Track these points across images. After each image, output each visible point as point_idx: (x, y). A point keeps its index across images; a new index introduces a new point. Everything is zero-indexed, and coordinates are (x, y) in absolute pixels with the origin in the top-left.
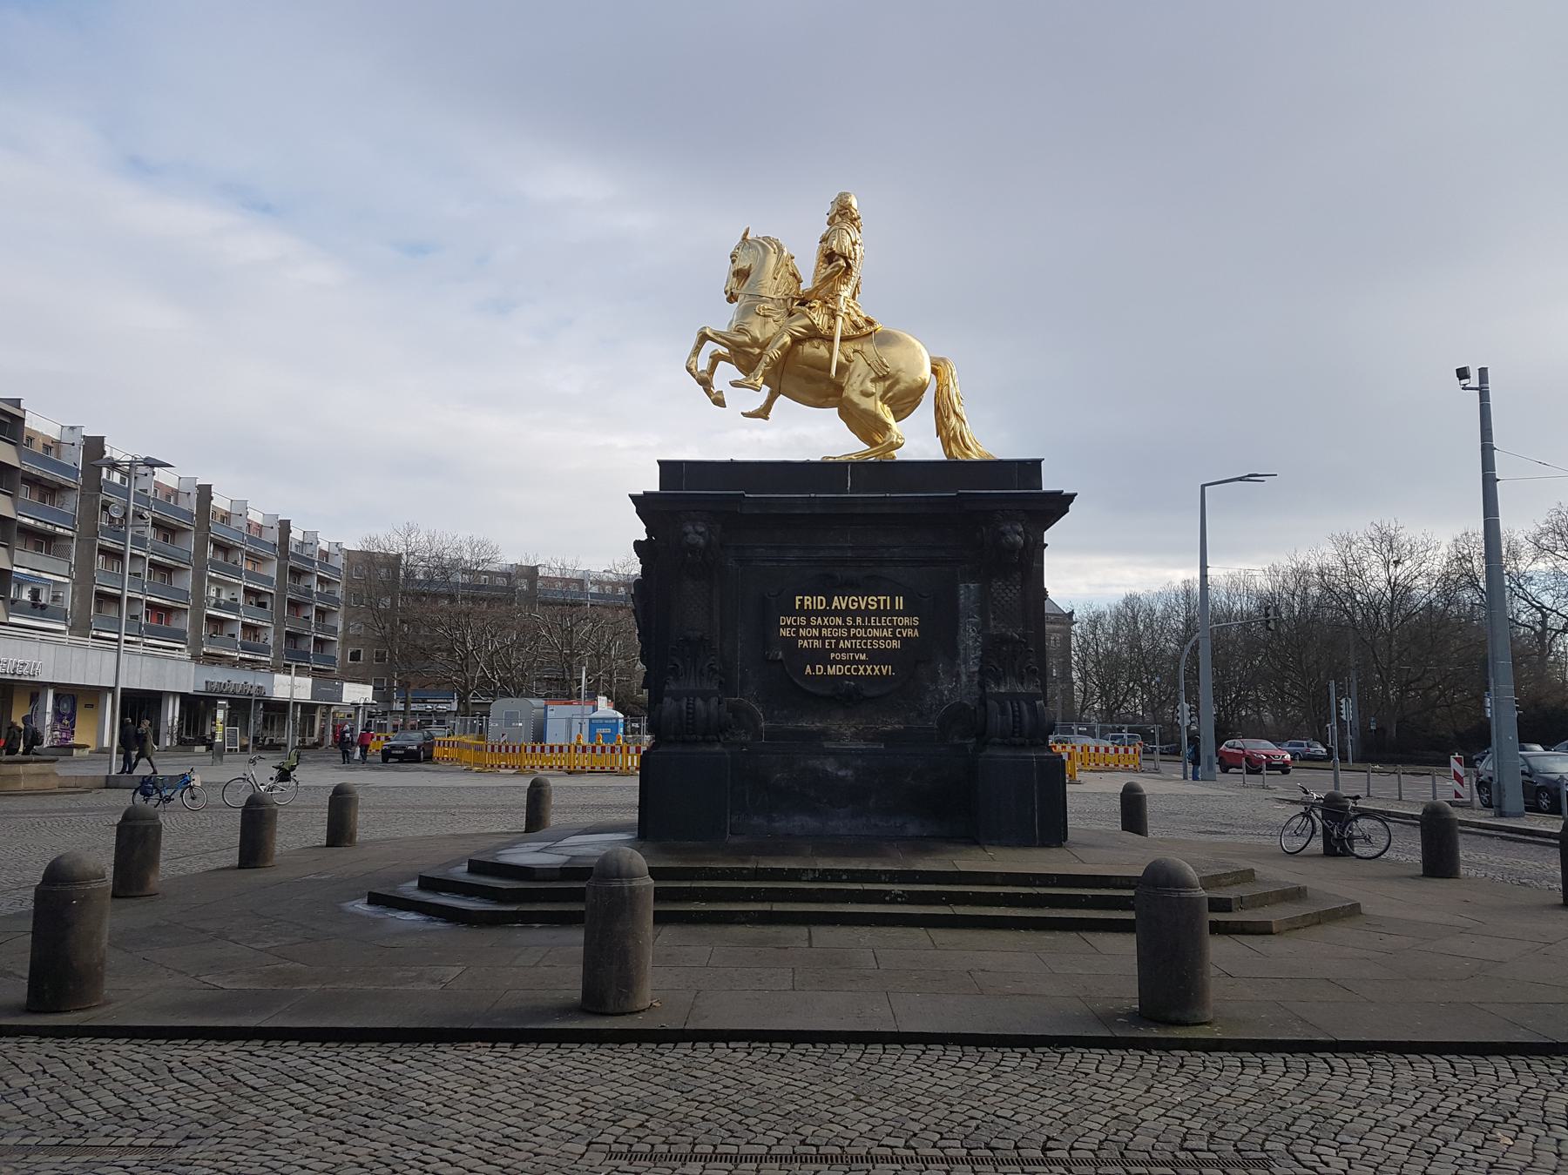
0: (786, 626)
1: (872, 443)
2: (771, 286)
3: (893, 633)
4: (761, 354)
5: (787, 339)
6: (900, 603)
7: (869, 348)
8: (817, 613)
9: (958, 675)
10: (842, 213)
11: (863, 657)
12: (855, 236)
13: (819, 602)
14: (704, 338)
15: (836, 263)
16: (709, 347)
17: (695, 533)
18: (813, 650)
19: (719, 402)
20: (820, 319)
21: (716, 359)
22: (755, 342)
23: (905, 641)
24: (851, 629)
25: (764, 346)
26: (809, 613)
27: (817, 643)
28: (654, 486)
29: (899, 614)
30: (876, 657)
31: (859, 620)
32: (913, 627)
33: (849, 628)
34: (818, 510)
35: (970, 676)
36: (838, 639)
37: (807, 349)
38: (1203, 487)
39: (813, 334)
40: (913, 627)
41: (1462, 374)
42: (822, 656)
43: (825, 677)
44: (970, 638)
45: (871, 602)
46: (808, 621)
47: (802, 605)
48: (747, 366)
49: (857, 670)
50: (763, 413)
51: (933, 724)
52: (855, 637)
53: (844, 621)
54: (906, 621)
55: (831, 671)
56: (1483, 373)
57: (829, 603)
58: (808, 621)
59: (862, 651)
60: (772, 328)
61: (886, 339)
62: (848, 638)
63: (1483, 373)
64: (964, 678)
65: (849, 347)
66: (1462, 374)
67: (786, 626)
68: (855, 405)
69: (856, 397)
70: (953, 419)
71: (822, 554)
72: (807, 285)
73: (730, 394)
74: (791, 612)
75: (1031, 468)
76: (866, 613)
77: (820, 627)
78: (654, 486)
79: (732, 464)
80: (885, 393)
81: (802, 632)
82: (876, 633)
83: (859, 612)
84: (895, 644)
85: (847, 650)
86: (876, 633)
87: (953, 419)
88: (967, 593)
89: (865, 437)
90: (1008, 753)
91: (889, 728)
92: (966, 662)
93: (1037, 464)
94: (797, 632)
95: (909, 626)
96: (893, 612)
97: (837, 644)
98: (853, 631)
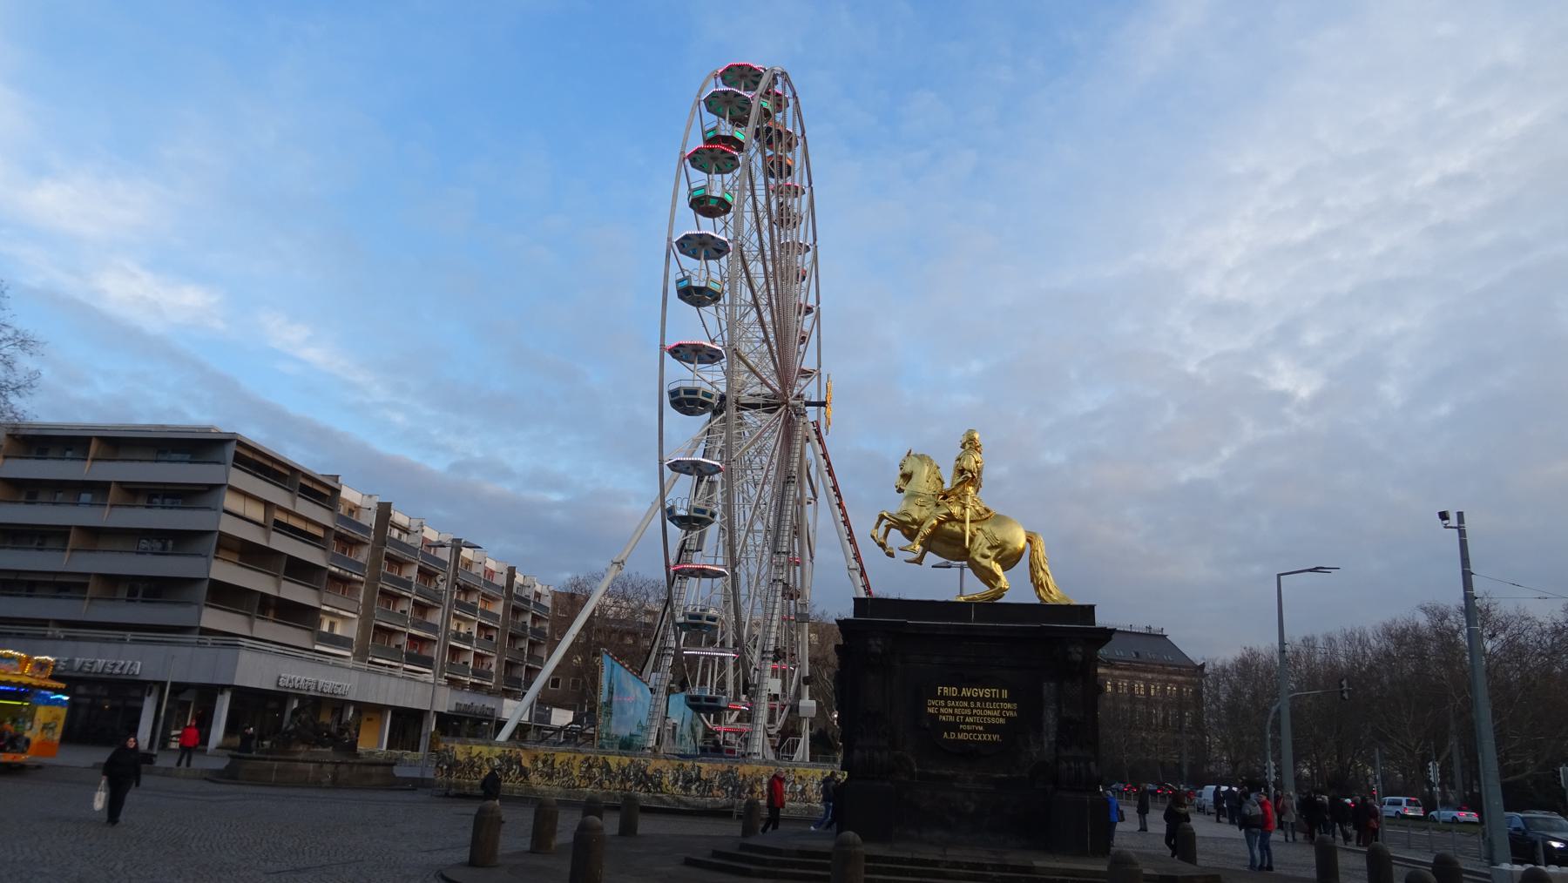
1: (992, 586)
2: (923, 482)
4: (918, 531)
6: (1005, 694)
7: (986, 527)
8: (952, 698)
10: (970, 444)
12: (977, 457)
13: (953, 691)
14: (882, 518)
16: (885, 522)
17: (876, 645)
18: (948, 723)
19: (891, 555)
20: (956, 510)
21: (888, 528)
22: (914, 521)
23: (1008, 718)
25: (920, 524)
27: (951, 719)
28: (851, 616)
29: (1004, 701)
30: (990, 728)
37: (947, 526)
39: (951, 517)
41: (1444, 516)
42: (954, 727)
43: (956, 741)
44: (1050, 718)
45: (987, 692)
48: (911, 536)
50: (919, 561)
55: (961, 736)
56: (1460, 515)
60: (925, 513)
61: (1000, 520)
63: (1460, 515)
65: (974, 526)
66: (1444, 516)
69: (978, 559)
72: (947, 486)
73: (896, 552)
75: (1088, 611)
76: (983, 700)
78: (851, 616)
79: (899, 601)
83: (978, 699)
84: (1002, 721)
87: (1041, 574)
88: (1049, 688)
89: (986, 581)
93: (1092, 608)
96: (1001, 700)
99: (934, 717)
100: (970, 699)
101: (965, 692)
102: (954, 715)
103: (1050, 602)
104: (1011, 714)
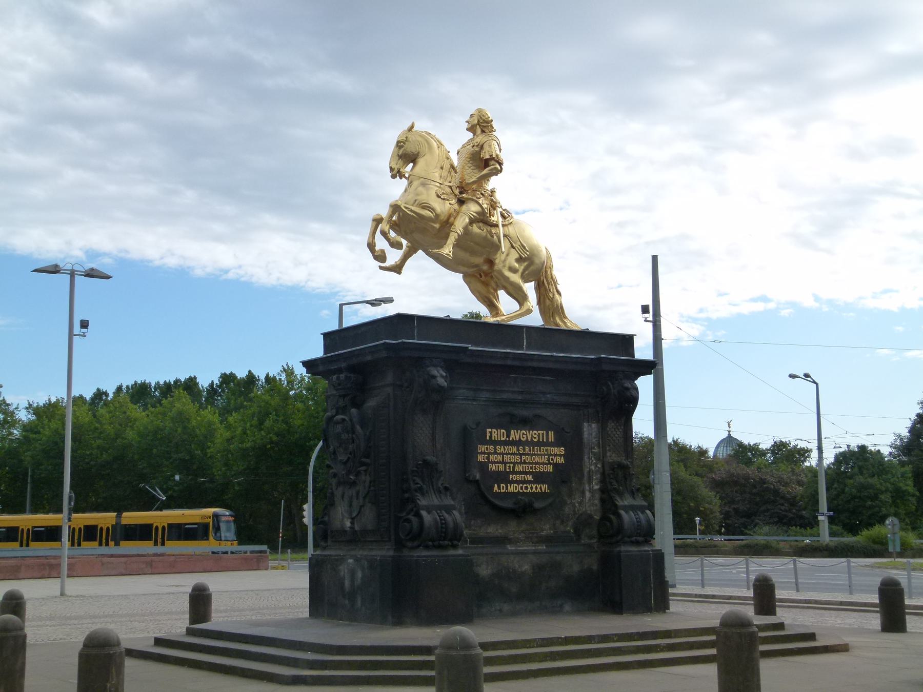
0: (482, 453)
3: (548, 460)
5: (467, 220)
6: (551, 434)
9: (583, 493)
11: (530, 478)
15: (485, 163)
18: (499, 473)
23: (556, 465)
24: (521, 457)
26: (496, 443)
30: (539, 478)
31: (527, 448)
32: (560, 455)
33: (521, 455)
34: (509, 362)
35: (592, 491)
36: (514, 463)
38: (341, 306)
40: (560, 455)
42: (503, 477)
43: (508, 495)
44: (591, 465)
46: (495, 449)
47: (491, 437)
49: (526, 488)
50: (397, 269)
51: (570, 528)
52: (525, 463)
53: (518, 450)
54: (556, 450)
55: (512, 488)
57: (508, 436)
58: (495, 449)
59: (529, 473)
62: (521, 463)
64: (588, 494)
67: (482, 453)
68: (507, 279)
70: (557, 296)
71: (505, 396)
74: (485, 442)
77: (503, 454)
80: (524, 270)
81: (492, 458)
82: (537, 459)
84: (550, 468)
85: (520, 473)
86: (537, 459)
88: (590, 431)
90: (634, 549)
91: (544, 533)
92: (590, 482)
94: (488, 458)
95: (558, 454)
97: (514, 468)
98: (524, 458)
99: (483, 466)
100: (518, 443)
101: (515, 435)
102: (504, 463)
103: (563, 327)
104: (561, 460)
